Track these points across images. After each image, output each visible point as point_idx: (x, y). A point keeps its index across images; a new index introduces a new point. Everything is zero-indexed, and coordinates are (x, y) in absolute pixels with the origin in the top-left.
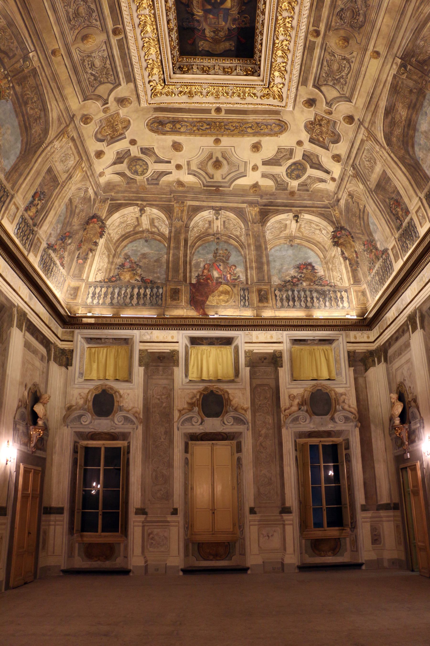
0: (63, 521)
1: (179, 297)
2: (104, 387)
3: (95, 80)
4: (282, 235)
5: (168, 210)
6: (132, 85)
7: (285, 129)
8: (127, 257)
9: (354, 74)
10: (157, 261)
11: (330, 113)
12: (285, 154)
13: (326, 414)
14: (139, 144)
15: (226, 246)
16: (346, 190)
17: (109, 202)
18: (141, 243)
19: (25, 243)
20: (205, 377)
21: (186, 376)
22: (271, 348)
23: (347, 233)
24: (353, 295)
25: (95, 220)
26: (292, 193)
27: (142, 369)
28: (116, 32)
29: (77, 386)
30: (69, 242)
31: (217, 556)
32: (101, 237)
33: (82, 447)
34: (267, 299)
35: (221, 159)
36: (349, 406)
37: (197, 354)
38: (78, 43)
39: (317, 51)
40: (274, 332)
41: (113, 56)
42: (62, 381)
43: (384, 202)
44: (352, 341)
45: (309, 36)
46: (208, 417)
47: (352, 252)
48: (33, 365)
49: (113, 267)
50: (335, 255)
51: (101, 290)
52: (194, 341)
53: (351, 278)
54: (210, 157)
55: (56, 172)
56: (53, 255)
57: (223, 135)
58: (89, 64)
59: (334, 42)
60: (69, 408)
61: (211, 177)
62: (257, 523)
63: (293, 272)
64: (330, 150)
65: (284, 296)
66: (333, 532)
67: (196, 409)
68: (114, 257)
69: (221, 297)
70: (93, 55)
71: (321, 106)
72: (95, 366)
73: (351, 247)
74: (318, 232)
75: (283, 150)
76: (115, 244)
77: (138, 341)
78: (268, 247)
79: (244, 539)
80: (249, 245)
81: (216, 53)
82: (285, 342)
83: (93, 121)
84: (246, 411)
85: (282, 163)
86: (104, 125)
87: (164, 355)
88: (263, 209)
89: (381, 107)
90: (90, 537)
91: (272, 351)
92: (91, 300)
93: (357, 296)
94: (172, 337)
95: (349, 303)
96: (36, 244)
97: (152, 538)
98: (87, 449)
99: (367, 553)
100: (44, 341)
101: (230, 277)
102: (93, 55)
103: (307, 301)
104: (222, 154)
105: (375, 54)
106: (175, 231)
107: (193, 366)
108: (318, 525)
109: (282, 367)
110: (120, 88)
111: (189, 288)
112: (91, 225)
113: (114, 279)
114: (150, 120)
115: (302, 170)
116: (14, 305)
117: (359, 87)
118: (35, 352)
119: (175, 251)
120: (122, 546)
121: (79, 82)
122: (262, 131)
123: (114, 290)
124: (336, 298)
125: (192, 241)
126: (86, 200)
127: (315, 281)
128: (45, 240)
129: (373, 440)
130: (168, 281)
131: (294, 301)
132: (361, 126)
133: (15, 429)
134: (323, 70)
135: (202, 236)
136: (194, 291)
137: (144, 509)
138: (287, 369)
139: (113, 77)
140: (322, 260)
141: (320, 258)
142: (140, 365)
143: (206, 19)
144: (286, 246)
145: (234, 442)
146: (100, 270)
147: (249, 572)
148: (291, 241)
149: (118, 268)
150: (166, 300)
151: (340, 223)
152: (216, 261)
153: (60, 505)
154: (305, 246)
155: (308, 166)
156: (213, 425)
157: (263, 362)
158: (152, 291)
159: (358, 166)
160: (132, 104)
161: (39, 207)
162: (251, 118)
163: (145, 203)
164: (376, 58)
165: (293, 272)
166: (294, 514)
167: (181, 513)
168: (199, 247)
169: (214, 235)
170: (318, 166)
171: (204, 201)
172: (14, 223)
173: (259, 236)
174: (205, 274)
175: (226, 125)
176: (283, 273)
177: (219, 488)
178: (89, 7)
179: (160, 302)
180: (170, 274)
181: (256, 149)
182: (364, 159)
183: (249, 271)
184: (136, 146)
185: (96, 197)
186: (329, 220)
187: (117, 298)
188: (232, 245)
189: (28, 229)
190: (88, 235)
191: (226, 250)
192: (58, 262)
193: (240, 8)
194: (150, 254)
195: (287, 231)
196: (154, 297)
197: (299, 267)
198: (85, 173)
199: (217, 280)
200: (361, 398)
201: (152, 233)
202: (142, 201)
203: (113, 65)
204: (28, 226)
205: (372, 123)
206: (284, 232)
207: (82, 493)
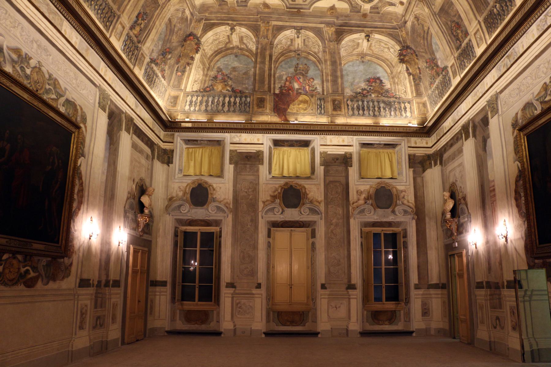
0: (166, 292)
2: (200, 182)
4: (355, 52)
5: (255, 29)
8: (219, 70)
10: (246, 73)
13: (388, 208)
15: (305, 62)
17: (204, 22)
19: (131, 58)
20: (285, 174)
21: (270, 173)
23: (412, 52)
24: (415, 106)
25: (192, 37)
26: (365, 15)
27: (232, 166)
29: (177, 181)
30: (169, 56)
31: (293, 323)
32: (197, 52)
33: (181, 231)
34: (340, 108)
36: (408, 202)
37: (279, 154)
40: (346, 137)
42: (165, 176)
43: (446, 24)
44: (413, 146)
46: (288, 208)
47: (416, 69)
48: (139, 163)
49: (207, 78)
50: (400, 71)
51: (197, 99)
52: (277, 143)
53: (414, 92)
56: (155, 68)
60: (171, 199)
62: (327, 296)
63: (363, 85)
65: (355, 106)
66: (390, 306)
67: (278, 201)
68: (208, 70)
69: (301, 106)
72: (192, 164)
74: (386, 50)
76: (209, 59)
77: (229, 142)
78: (342, 62)
79: (316, 309)
80: (326, 61)
82: (355, 145)
84: (320, 203)
87: (251, 154)
90: (189, 305)
91: (344, 153)
93: (419, 107)
94: (258, 140)
96: (140, 59)
97: (240, 307)
98: (186, 233)
99: (417, 322)
100: (149, 142)
103: (375, 110)
106: (262, 48)
107: (276, 164)
108: (378, 299)
109: (351, 166)
111: (273, 97)
112: (188, 42)
113: (208, 89)
116: (123, 112)
118: (141, 151)
120: (215, 312)
123: (208, 98)
124: (400, 109)
126: (184, 20)
128: (148, 55)
129: (427, 231)
131: (363, 110)
133: (125, 217)
137: (233, 283)
138: (355, 168)
141: (387, 73)
142: (230, 163)
144: (358, 62)
145: (309, 229)
146: (196, 81)
147: (319, 336)
148: (362, 57)
150: (253, 107)
151: (406, 43)
152: (297, 74)
153: (164, 280)
154: (375, 63)
156: (292, 214)
157: (335, 162)
158: (241, 99)
161: (142, 26)
163: (235, 23)
165: (363, 85)
166: (358, 290)
167: (264, 288)
168: (281, 62)
172: (121, 40)
173: (334, 53)
177: (296, 267)
179: (248, 109)
180: (257, 85)
186: (396, 39)
188: (311, 60)
189: (133, 46)
191: (306, 65)
192: (160, 75)
196: (243, 105)
197: (369, 81)
199: (297, 91)
200: (418, 194)
201: (241, 49)
204: (133, 43)
206: (357, 50)
207: (182, 269)
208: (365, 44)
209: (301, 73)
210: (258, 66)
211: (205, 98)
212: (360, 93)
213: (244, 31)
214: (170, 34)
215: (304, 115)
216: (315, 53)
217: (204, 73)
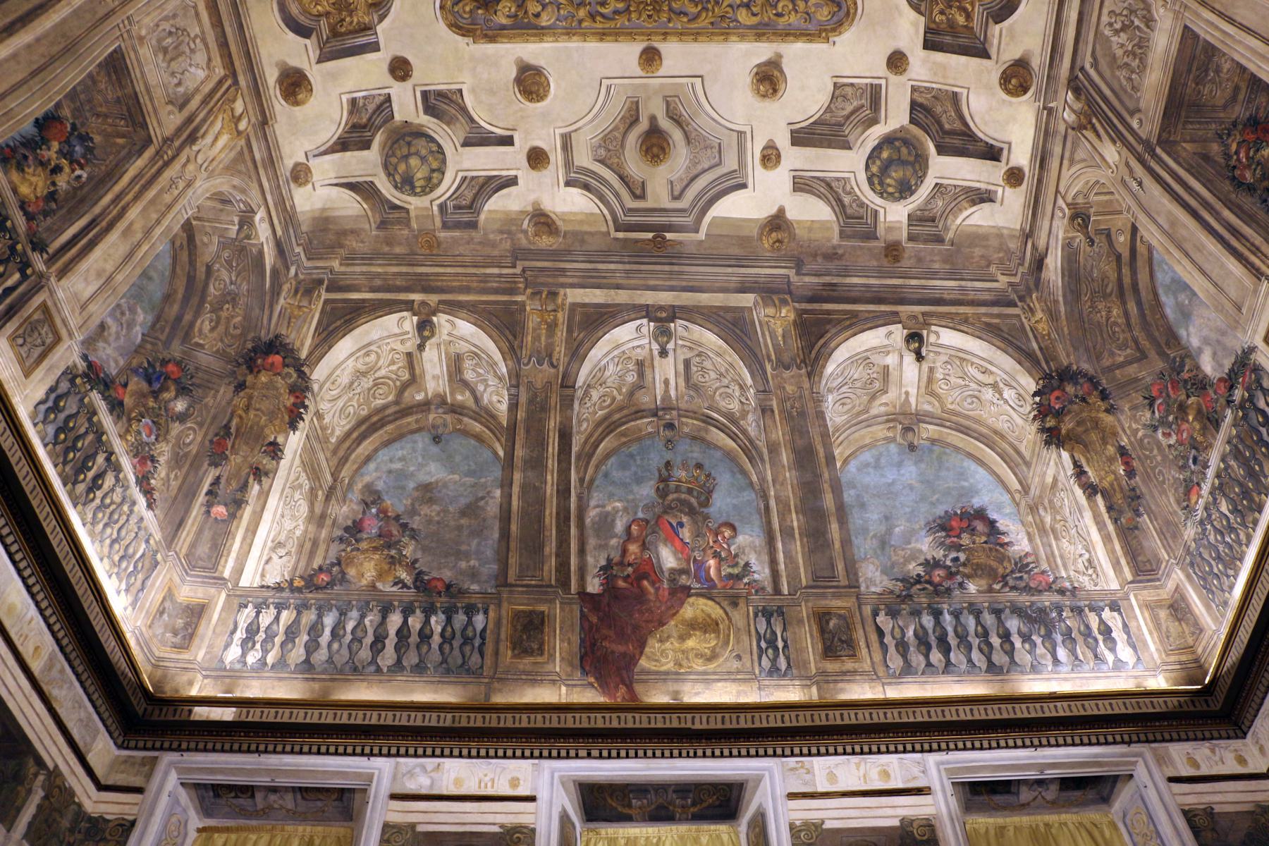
1: (542, 644)
5: (505, 324)
7: (848, 13)
8: (372, 498)
10: (471, 510)
12: (855, 104)
15: (696, 454)
16: (1060, 202)
17: (325, 295)
18: (420, 445)
22: (890, 812)
24: (1142, 621)
25: (277, 359)
26: (893, 251)
30: (180, 406)
32: (293, 427)
34: (850, 645)
35: (665, 124)
47: (1111, 460)
50: (1055, 480)
51: (277, 618)
53: (1123, 561)
54: (632, 118)
55: (140, 88)
56: (106, 419)
57: (665, 36)
63: (926, 546)
64: (993, 52)
65: (910, 633)
68: (328, 498)
69: (691, 643)
73: (1104, 442)
74: (988, 394)
75: (849, 90)
76: (335, 452)
78: (837, 452)
80: (773, 449)
82: (936, 786)
85: (851, 138)
88: (806, 311)
91: (896, 823)
92: (239, 651)
93: (1156, 620)
95: (1134, 648)
101: (719, 570)
103: (990, 645)
104: (667, 102)
106: (531, 401)
111: (576, 608)
112: (263, 378)
113: (324, 578)
115: (912, 164)
119: (529, 474)
122: (781, 20)
123: (320, 616)
124: (1087, 633)
125: (583, 437)
126: (243, 254)
127: (1004, 577)
128: (79, 337)
130: (506, 585)
135: (617, 416)
136: (594, 619)
140: (1017, 496)
141: (1009, 491)
144: (893, 447)
146: (280, 545)
148: (907, 429)
149: (341, 539)
150: (497, 653)
151: (1055, 359)
152: (668, 509)
154: (957, 449)
155: (932, 149)
158: (449, 620)
159: (1092, 72)
163: (433, 299)
165: (926, 546)
168: (607, 456)
169: (655, 415)
170: (964, 142)
171: (618, 287)
173: (802, 414)
174: (631, 558)
176: (895, 548)
179: (475, 658)
180: (513, 560)
181: (767, 84)
182: (1107, 32)
183: (780, 545)
184: (408, 84)
185: (279, 265)
186: (1018, 348)
187: (329, 645)
188: (717, 447)
190: (252, 414)
191: (699, 466)
194: (445, 485)
195: (892, 395)
196: (456, 644)
197: (945, 526)
198: (243, 142)
199: (672, 580)
201: (457, 409)
202: (427, 290)
206: (884, 399)
208: (910, 371)
209: (682, 501)
210: (517, 477)
211: (309, 617)
212: (918, 579)
213: (462, 331)
214: (186, 299)
215: (705, 675)
216: (730, 416)
217: (312, 510)
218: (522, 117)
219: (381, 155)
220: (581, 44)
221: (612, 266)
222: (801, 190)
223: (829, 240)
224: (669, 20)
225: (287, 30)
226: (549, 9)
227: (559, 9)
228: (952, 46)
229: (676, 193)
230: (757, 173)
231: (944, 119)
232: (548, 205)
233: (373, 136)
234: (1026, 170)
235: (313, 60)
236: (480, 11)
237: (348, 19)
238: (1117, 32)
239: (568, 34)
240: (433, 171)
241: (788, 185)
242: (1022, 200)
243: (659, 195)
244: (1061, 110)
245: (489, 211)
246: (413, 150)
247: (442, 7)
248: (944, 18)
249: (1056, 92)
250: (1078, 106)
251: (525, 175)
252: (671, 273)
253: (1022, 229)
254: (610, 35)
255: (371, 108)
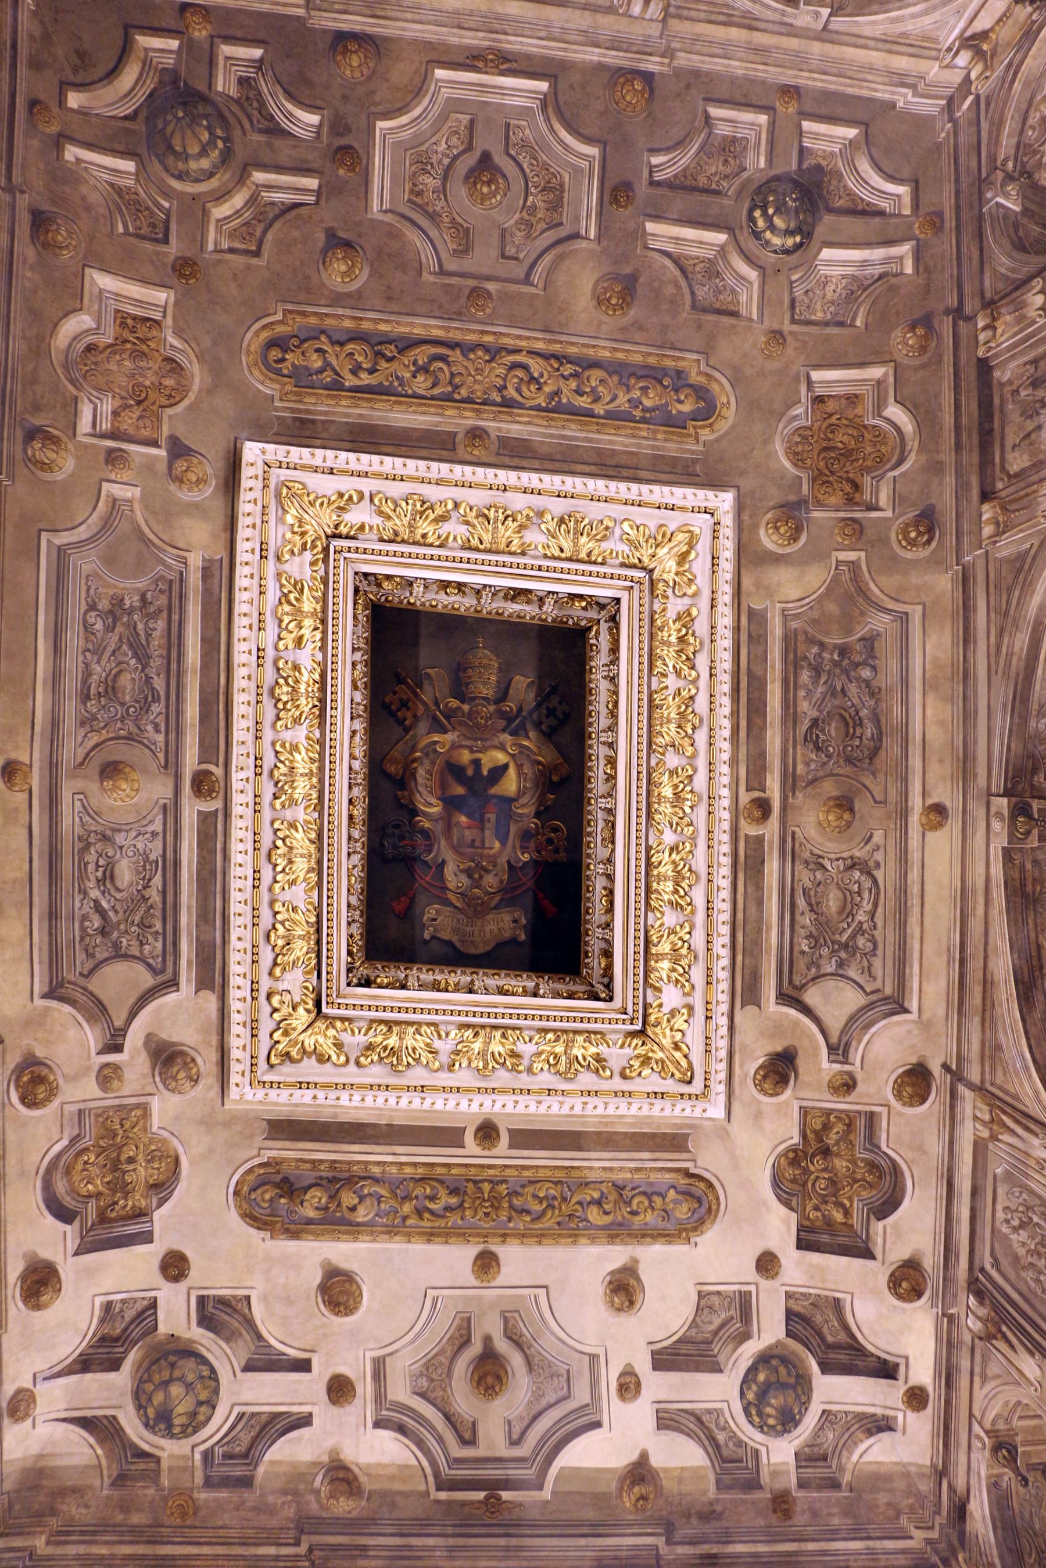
3: (103, 932)
6: (210, 1001)
7: (709, 1210)
9: (891, 904)
11: (848, 1085)
12: (723, 1316)
14: (196, 1276)
16: (977, 1429)
26: (782, 1503)
28: (202, 785)
35: (502, 1345)
38: (86, 777)
39: (772, 867)
41: (177, 864)
45: (742, 822)
54: (462, 1339)
58: (98, 866)
59: (812, 822)
61: (468, 1437)
64: (878, 1251)
70: (120, 839)
71: (819, 1066)
75: (715, 1299)
81: (473, 951)
83: (56, 1103)
85: (721, 1358)
86: (87, 1142)
89: (1002, 977)
102: (120, 839)
104: (505, 1318)
105: (932, 816)
110: (171, 998)
114: (250, 1171)
115: (794, 1388)
117: (917, 946)
121: (52, 915)
122: (638, 1220)
132: (961, 1088)
134: (797, 927)
139: (159, 945)
143: (448, 828)
159: (994, 1273)
160: (200, 1086)
162: (596, 1163)
164: (940, 825)
170: (852, 1358)
175: (516, 1193)
178: (148, 679)
181: (623, 1293)
182: (1005, 1229)
184: (182, 1286)
193: (541, 801)
203: (170, 898)
205: (991, 1053)
218: (325, 1335)
219: (133, 1379)
220: (404, 1246)
221: (431, 1541)
222: (667, 1427)
223: (704, 1492)
224: (510, 1220)
225: (46, 1213)
226: (368, 1201)
227: (379, 1203)
228: (831, 1246)
229: (515, 1436)
230: (614, 1408)
231: (825, 1330)
232: (350, 1455)
233: (126, 1352)
234: (930, 1389)
235: (70, 1250)
236: (283, 1201)
237: (121, 1202)
238: (1015, 1229)
239: (389, 1233)
240: (200, 1403)
241: (651, 1422)
242: (930, 1427)
243: (493, 1440)
244: (963, 1316)
245: (272, 1463)
246: (177, 1373)
247: (236, 1193)
248: (819, 1214)
249: (955, 1296)
250: (982, 1312)
251: (322, 1411)
252: (507, 1548)
253: (933, 1466)
254: (439, 1235)
255: (129, 1314)
